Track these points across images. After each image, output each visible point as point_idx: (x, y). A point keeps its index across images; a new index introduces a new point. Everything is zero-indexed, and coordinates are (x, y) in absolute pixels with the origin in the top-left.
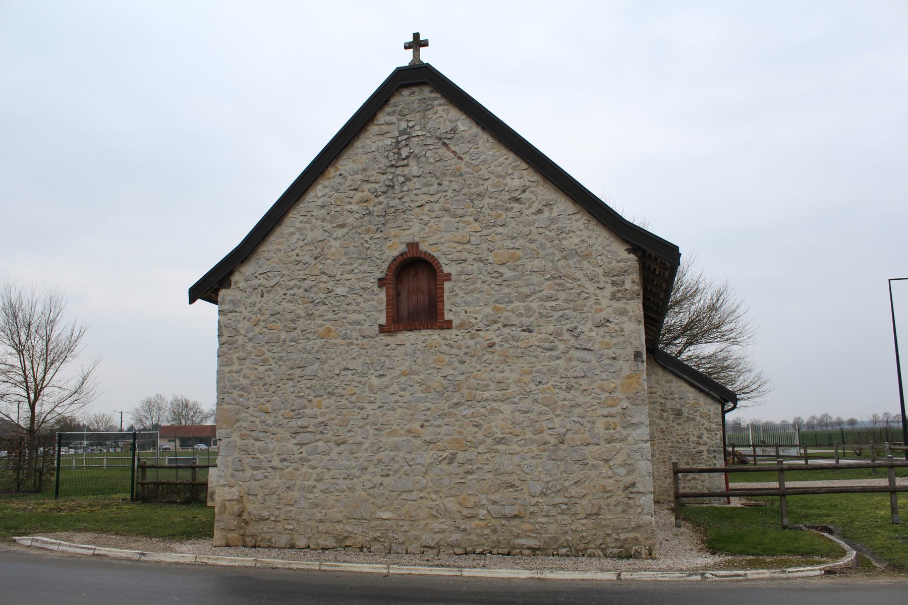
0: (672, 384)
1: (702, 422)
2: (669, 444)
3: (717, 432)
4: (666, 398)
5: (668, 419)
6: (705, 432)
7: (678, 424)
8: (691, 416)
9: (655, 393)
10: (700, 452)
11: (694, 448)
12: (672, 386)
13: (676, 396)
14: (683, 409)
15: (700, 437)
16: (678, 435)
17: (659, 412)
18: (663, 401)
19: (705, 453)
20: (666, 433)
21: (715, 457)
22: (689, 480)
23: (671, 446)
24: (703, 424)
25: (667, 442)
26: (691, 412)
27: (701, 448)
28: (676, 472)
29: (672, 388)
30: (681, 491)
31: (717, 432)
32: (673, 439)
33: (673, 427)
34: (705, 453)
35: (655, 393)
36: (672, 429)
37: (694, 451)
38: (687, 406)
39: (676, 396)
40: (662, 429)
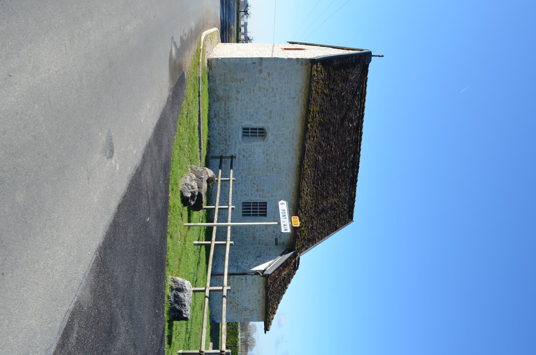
0: (274, 256)
1: (254, 263)
2: (242, 254)
3: (248, 268)
4: (267, 254)
5: (255, 253)
6: (248, 264)
7: (253, 257)
8: (257, 260)
9: (269, 250)
10: (238, 263)
11: (240, 261)
12: (273, 256)
13: (268, 256)
14: (261, 258)
15: (246, 263)
16: (247, 257)
17: (260, 252)
18: (265, 253)
19: (237, 264)
20: (248, 253)
21: (235, 267)
22: (223, 259)
23: (241, 255)
24: (253, 264)
25: (244, 254)
26: (259, 261)
27: (240, 264)
28: (232, 157)
29: (272, 256)
30: (223, 160)
31: (248, 268)
32: (245, 256)
33: (252, 255)
34: (237, 264)
35: (269, 250)
36: (251, 255)
37: (239, 261)
38: (263, 259)
39: (268, 256)
40: (251, 252)
